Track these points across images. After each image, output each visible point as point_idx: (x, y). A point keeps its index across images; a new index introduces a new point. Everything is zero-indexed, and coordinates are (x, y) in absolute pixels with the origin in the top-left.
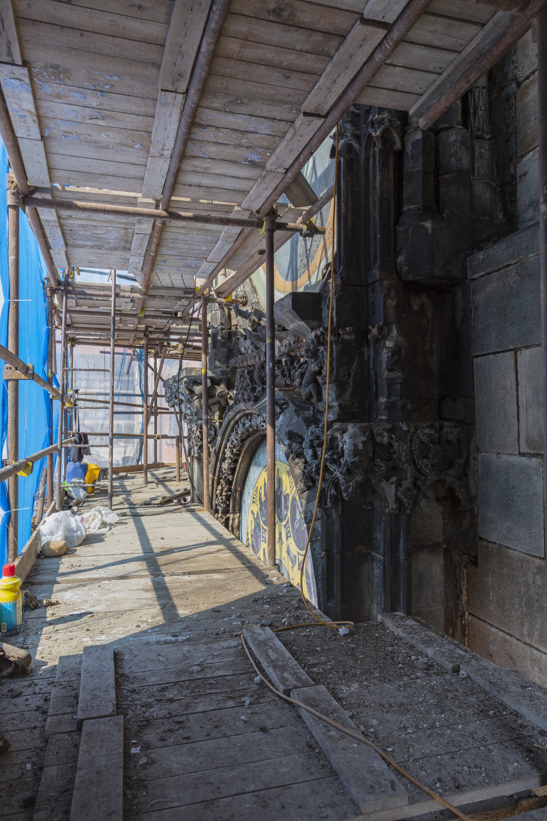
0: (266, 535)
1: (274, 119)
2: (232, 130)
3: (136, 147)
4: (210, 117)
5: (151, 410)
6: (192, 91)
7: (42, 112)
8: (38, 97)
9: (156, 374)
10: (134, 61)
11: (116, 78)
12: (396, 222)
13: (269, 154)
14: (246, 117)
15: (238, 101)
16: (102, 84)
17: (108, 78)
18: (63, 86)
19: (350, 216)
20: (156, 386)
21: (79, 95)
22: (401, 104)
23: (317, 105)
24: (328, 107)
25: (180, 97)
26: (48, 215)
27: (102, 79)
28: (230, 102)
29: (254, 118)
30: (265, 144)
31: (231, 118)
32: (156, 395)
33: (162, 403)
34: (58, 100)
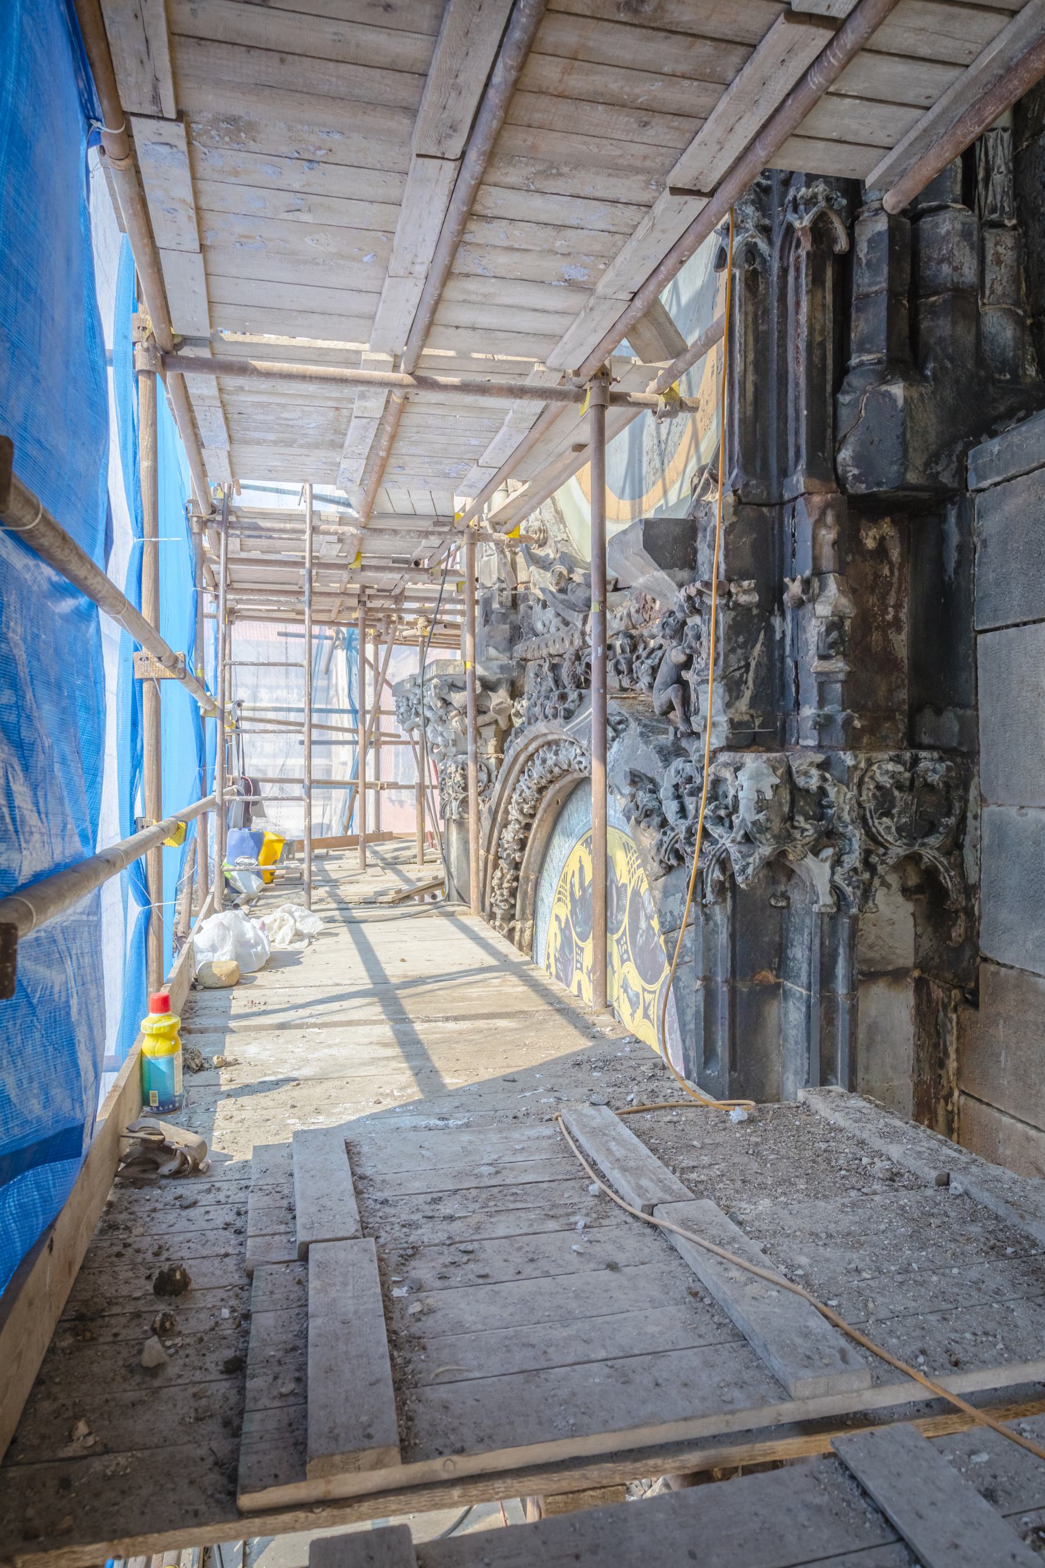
3: (366, 259)
4: (499, 202)
6: (472, 156)
7: (204, 202)
8: (198, 175)
10: (371, 105)
11: (337, 137)
12: (837, 387)
15: (552, 170)
16: (311, 149)
17: (324, 136)
18: (244, 154)
19: (751, 378)
21: (269, 170)
22: (851, 167)
25: (450, 167)
27: (313, 138)
30: (597, 247)
31: (537, 202)
32: (378, 711)
33: (389, 724)
34: (233, 180)
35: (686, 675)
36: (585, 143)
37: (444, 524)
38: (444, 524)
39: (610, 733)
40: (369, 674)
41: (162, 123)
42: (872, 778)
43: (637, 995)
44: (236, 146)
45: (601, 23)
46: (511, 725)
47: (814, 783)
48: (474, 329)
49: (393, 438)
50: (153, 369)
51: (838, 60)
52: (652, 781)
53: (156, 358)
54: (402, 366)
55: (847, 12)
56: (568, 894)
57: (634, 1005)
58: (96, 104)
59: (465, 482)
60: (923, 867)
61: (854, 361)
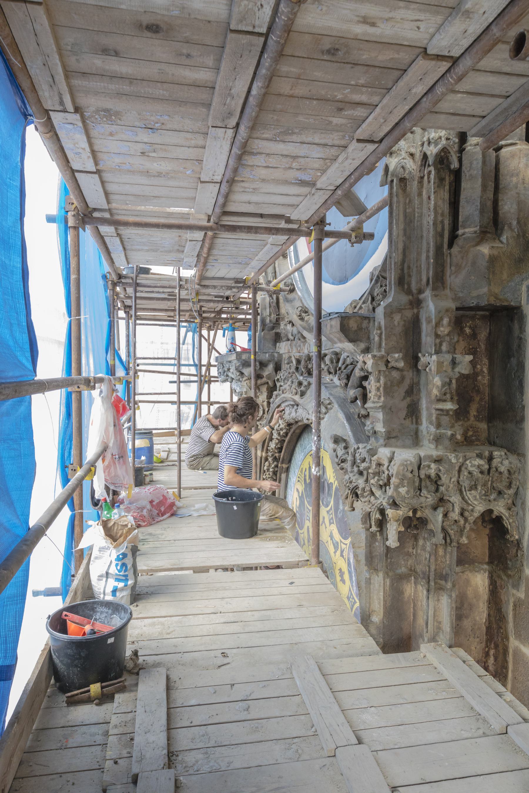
0: (311, 515)
1: (325, 145)
2: (282, 155)
3: (188, 173)
4: (260, 146)
5: (205, 379)
7: (96, 148)
8: (91, 136)
9: (209, 344)
10: (183, 102)
11: (166, 117)
12: (451, 245)
13: (319, 174)
14: (297, 144)
15: (289, 132)
16: (153, 123)
17: (159, 117)
19: (401, 238)
20: (209, 357)
23: (371, 133)
24: (382, 134)
25: (230, 133)
26: (105, 229)
27: (152, 118)
28: (281, 132)
29: (305, 145)
30: (316, 166)
32: (209, 365)
35: (365, 384)
36: (306, 118)
37: (241, 283)
38: (240, 283)
39: (323, 410)
40: (205, 344)
41: (67, 114)
42: (466, 468)
43: (337, 543)
44: (110, 123)
45: (313, 61)
46: (275, 385)
47: (432, 472)
48: (250, 203)
49: (210, 249)
50: (77, 225)
51: (454, 80)
52: (345, 441)
53: (79, 220)
54: (212, 220)
55: (460, 54)
56: (303, 479)
57: (336, 547)
58: (29, 108)
59: (250, 266)
60: (494, 517)
61: (460, 232)
